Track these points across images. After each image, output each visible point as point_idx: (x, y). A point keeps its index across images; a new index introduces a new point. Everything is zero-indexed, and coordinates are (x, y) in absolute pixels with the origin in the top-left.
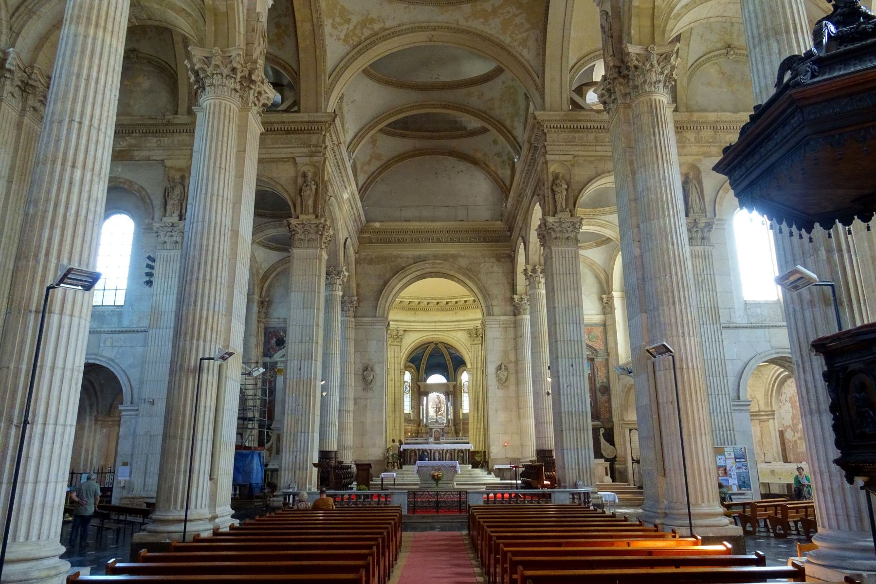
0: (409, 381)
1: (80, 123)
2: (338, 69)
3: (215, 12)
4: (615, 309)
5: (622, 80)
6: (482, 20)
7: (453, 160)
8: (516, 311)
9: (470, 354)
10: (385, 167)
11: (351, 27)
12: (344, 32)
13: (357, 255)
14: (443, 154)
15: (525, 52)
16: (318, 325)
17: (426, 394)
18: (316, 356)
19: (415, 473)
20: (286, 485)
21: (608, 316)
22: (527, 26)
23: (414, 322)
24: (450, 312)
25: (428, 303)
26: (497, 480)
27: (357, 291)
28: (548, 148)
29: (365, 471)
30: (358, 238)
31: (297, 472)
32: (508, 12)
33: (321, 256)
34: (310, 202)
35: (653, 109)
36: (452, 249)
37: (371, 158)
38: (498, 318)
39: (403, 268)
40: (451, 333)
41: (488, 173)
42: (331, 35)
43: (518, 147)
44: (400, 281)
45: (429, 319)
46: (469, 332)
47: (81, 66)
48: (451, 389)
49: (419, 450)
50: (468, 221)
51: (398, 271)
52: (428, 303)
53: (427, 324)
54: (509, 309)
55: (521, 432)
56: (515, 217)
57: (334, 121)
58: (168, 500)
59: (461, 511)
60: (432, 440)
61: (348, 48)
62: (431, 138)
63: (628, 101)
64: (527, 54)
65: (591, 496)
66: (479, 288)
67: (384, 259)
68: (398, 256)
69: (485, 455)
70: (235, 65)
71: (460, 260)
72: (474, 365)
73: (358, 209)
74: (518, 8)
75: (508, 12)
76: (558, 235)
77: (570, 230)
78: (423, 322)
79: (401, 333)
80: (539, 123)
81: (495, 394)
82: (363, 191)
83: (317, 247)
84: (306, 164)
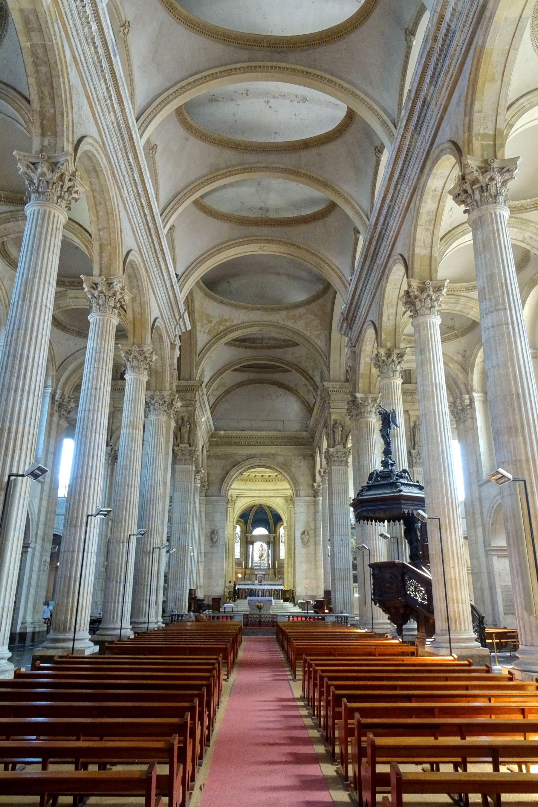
0: (239, 533)
1: (133, 469)
2: (204, 351)
3: (156, 372)
5: (355, 407)
6: (293, 321)
7: (274, 388)
8: (315, 495)
9: (286, 515)
10: (228, 392)
11: (213, 325)
12: (208, 329)
14: (268, 383)
15: (319, 343)
16: (190, 513)
17: (252, 543)
18: (189, 533)
19: (247, 604)
20: (170, 610)
22: (320, 327)
23: (244, 489)
24: (272, 483)
25: (255, 476)
26: (300, 610)
27: (208, 478)
28: (331, 404)
29: (217, 603)
30: (209, 441)
31: (177, 602)
32: (309, 318)
33: (192, 469)
34: (186, 436)
35: (368, 426)
36: (272, 450)
37: (219, 385)
38: (303, 498)
39: (239, 463)
40: (272, 499)
41: (298, 396)
42: (200, 331)
44: (237, 471)
45: (254, 488)
46: (286, 498)
47: (132, 446)
48: (272, 540)
49: (248, 589)
50: (284, 431)
51: (235, 464)
52: (255, 476)
53: (254, 492)
54: (311, 492)
55: (316, 578)
56: (315, 432)
57: (201, 385)
58: (139, 613)
59: (273, 626)
60: (256, 582)
61: (210, 338)
62: (260, 372)
63: (357, 418)
64: (320, 343)
65: (349, 619)
66: (290, 477)
67: (226, 456)
68: (236, 454)
69: (293, 593)
70: (166, 400)
71: (278, 457)
72: (289, 523)
73: (210, 425)
74: (315, 317)
75: (309, 318)
76: (336, 459)
77: (342, 456)
78: (251, 490)
79: (234, 498)
80: (326, 388)
81: (300, 551)
82: (213, 408)
83: (189, 464)
84: (184, 412)
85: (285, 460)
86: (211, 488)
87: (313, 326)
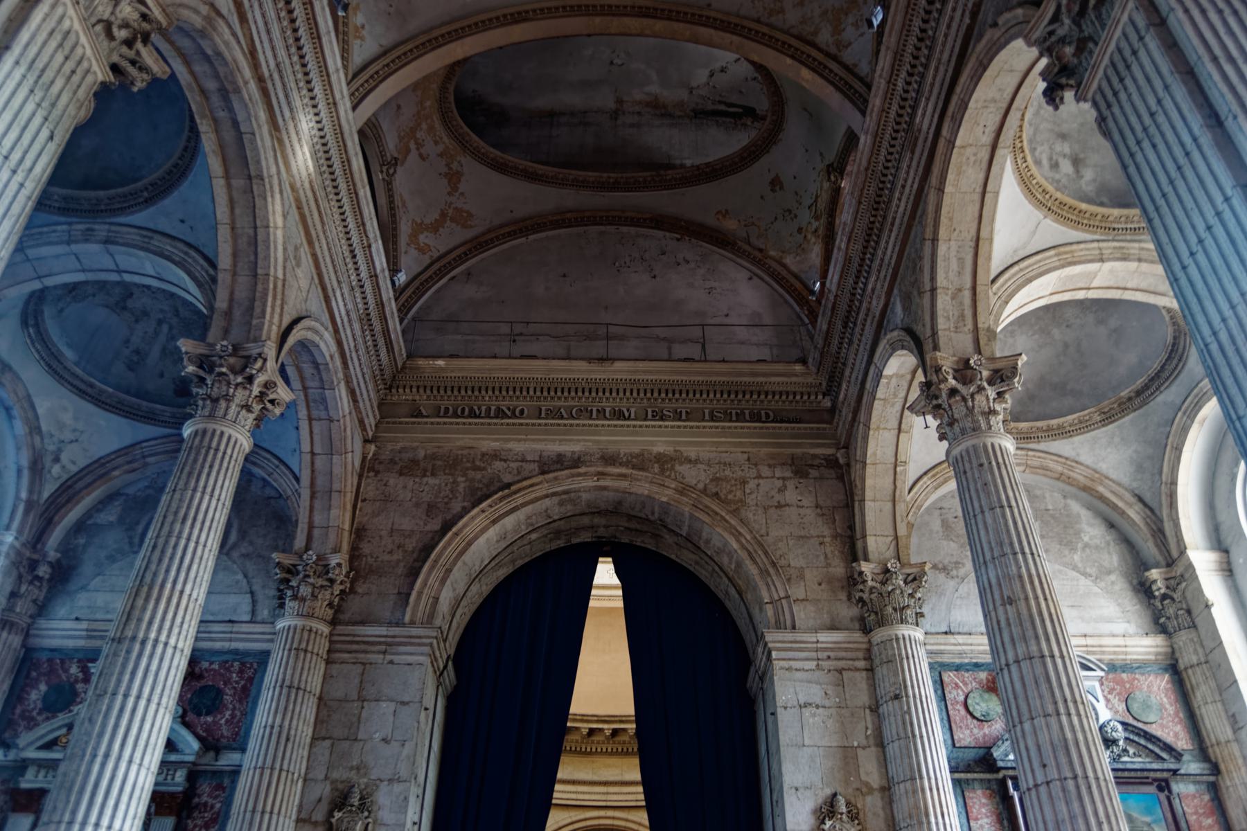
4: (1208, 607)
13: (373, 448)
21: (1183, 638)
30: (380, 405)
39: (508, 486)
43: (857, 85)
44: (494, 522)
54: (847, 612)
67: (452, 463)
85: (716, 480)
86: (361, 588)
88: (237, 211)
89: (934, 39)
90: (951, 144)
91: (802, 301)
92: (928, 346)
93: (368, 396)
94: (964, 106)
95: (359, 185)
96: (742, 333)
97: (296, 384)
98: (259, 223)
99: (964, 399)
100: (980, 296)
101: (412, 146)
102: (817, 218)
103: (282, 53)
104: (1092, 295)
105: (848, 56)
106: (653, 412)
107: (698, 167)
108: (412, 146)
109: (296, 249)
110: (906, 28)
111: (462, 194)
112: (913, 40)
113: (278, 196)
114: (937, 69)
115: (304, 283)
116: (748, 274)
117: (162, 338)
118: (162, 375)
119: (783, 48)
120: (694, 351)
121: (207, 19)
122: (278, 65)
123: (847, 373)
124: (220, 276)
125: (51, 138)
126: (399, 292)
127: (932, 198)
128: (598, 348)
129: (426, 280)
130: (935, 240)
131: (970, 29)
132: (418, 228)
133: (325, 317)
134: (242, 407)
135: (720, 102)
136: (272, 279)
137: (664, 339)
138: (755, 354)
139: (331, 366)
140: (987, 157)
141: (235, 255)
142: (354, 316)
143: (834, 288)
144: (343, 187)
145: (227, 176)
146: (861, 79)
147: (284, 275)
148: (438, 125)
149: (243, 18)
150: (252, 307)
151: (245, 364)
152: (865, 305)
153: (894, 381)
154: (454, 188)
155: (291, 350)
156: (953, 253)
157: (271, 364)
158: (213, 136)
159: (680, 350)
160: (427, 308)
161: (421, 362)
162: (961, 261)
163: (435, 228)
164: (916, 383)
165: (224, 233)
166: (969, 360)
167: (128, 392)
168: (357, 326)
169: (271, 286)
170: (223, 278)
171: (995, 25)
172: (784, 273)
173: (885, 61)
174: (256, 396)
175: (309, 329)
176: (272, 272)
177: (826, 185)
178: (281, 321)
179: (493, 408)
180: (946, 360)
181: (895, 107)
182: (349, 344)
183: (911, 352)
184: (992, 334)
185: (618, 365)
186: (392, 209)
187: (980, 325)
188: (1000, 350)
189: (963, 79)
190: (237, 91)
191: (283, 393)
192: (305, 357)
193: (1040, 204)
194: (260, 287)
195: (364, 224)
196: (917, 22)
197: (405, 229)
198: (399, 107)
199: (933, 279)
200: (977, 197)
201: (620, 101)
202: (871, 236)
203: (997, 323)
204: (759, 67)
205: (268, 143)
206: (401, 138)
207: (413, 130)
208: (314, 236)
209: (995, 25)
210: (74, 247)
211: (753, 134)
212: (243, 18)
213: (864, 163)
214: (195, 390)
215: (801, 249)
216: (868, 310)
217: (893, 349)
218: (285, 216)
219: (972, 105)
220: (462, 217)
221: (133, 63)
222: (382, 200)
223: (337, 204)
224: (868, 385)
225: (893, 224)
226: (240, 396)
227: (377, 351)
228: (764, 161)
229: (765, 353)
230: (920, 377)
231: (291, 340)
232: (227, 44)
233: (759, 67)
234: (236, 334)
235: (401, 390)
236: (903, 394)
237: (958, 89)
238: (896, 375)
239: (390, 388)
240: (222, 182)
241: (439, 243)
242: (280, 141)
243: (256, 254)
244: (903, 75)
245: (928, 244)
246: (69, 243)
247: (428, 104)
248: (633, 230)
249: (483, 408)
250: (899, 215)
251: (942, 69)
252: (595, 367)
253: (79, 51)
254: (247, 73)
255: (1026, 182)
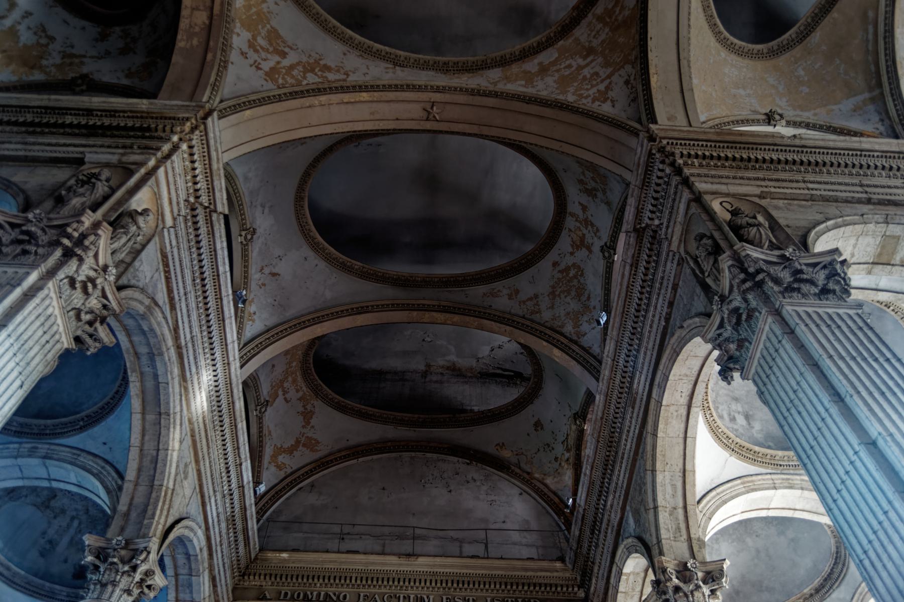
11: (286, 62)
12: (271, 64)
30: (234, 589)
87: (585, 78)
88: (147, 438)
89: (642, 334)
90: (659, 403)
91: (559, 512)
92: (655, 551)
93: (225, 581)
94: (666, 378)
95: (239, 420)
96: (516, 537)
97: (170, 571)
98: (161, 447)
99: (686, 595)
100: (690, 513)
101: (280, 393)
102: (568, 450)
103: (196, 330)
104: (772, 513)
105: (586, 341)
106: (447, 599)
107: (483, 412)
108: (280, 393)
109: (186, 465)
110: (623, 327)
111: (313, 427)
112: (628, 334)
113: (178, 427)
114: (645, 353)
115: (188, 492)
116: (520, 491)
117: (72, 531)
118: (66, 561)
119: (541, 336)
120: (479, 549)
121: (149, 308)
122: (192, 338)
123: (596, 570)
124: (126, 486)
125: (21, 386)
126: (258, 499)
127: (649, 440)
128: (407, 547)
129: (280, 490)
130: (654, 471)
131: (665, 328)
132: (279, 451)
133: (200, 519)
134: (125, 591)
135: (498, 368)
136: (164, 488)
137: (457, 539)
138: (526, 553)
139: (199, 557)
140: (685, 413)
141: (139, 470)
142: (222, 517)
143: (582, 503)
144: (227, 421)
145: (143, 413)
146: (594, 357)
147: (174, 485)
148: (299, 379)
149: (173, 307)
150: (145, 511)
151: (132, 555)
152: (606, 517)
153: (631, 577)
154: (307, 423)
155: (170, 544)
156: (667, 481)
157: (153, 556)
158: (138, 384)
159: (468, 549)
160: (278, 512)
161: (270, 555)
162: (674, 486)
163: (291, 451)
164: (648, 580)
165: (134, 454)
166: (687, 563)
167: (36, 575)
168: (223, 525)
169: (163, 494)
170: (128, 487)
171: (682, 327)
172: (546, 490)
173: (610, 347)
174: (137, 582)
175: (187, 527)
176: (165, 484)
177: (574, 427)
178: (166, 521)
179: (322, 593)
180: (670, 563)
181: (619, 377)
182: (215, 539)
183: (643, 556)
184: (702, 544)
185: (421, 560)
186: (260, 437)
187: (692, 536)
188: (710, 556)
189: (664, 360)
190: (161, 354)
191: (159, 580)
192: (181, 550)
193: (726, 446)
194: (154, 495)
195: (238, 448)
196: (630, 323)
197: (268, 451)
198: (273, 366)
199: (655, 500)
200: (681, 441)
201: (428, 366)
202: (608, 466)
203: (705, 536)
204: (524, 346)
205: (177, 390)
206: (272, 387)
207: (282, 382)
208: (201, 456)
209: (682, 327)
210: (20, 461)
211: (522, 390)
212: (173, 307)
213: (600, 414)
214: (89, 576)
215: (557, 473)
216: (609, 521)
217: (629, 552)
218: (181, 442)
219: (671, 377)
220: (311, 444)
221: (91, 336)
222: (254, 430)
223: (221, 434)
224: (612, 581)
225: (622, 458)
226: (124, 582)
227: (237, 545)
228: (530, 409)
229: (533, 553)
230: (651, 576)
231: (171, 537)
232: (159, 324)
233: (524, 346)
234: (130, 531)
235: (252, 577)
236: (639, 589)
237: (661, 367)
238: (633, 573)
239: (243, 575)
240: (139, 416)
241: (292, 462)
242: (186, 389)
243: (155, 469)
244: (623, 356)
245: (649, 473)
246: (16, 457)
247: (294, 364)
248: (435, 456)
249: (315, 593)
250: (627, 452)
251: (649, 353)
252: (403, 561)
253: (55, 328)
254: (170, 342)
255: (714, 431)
